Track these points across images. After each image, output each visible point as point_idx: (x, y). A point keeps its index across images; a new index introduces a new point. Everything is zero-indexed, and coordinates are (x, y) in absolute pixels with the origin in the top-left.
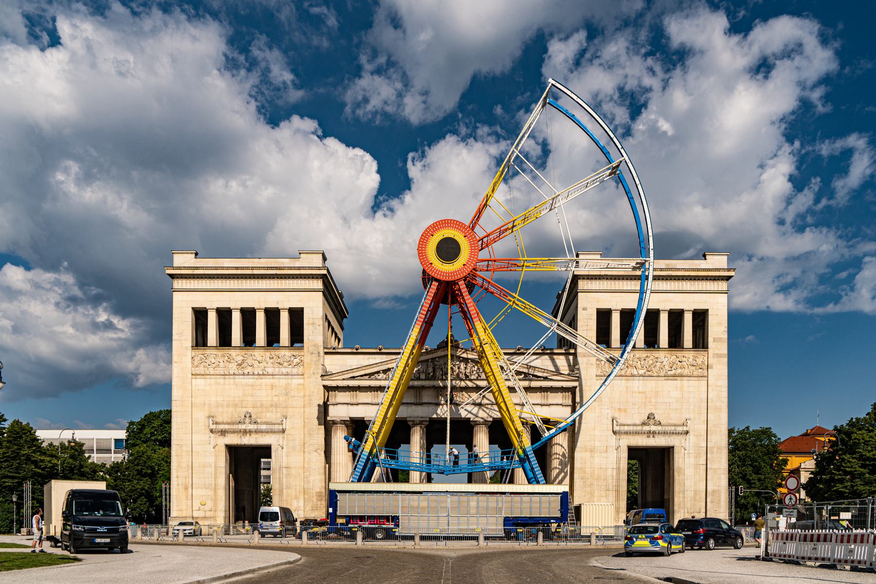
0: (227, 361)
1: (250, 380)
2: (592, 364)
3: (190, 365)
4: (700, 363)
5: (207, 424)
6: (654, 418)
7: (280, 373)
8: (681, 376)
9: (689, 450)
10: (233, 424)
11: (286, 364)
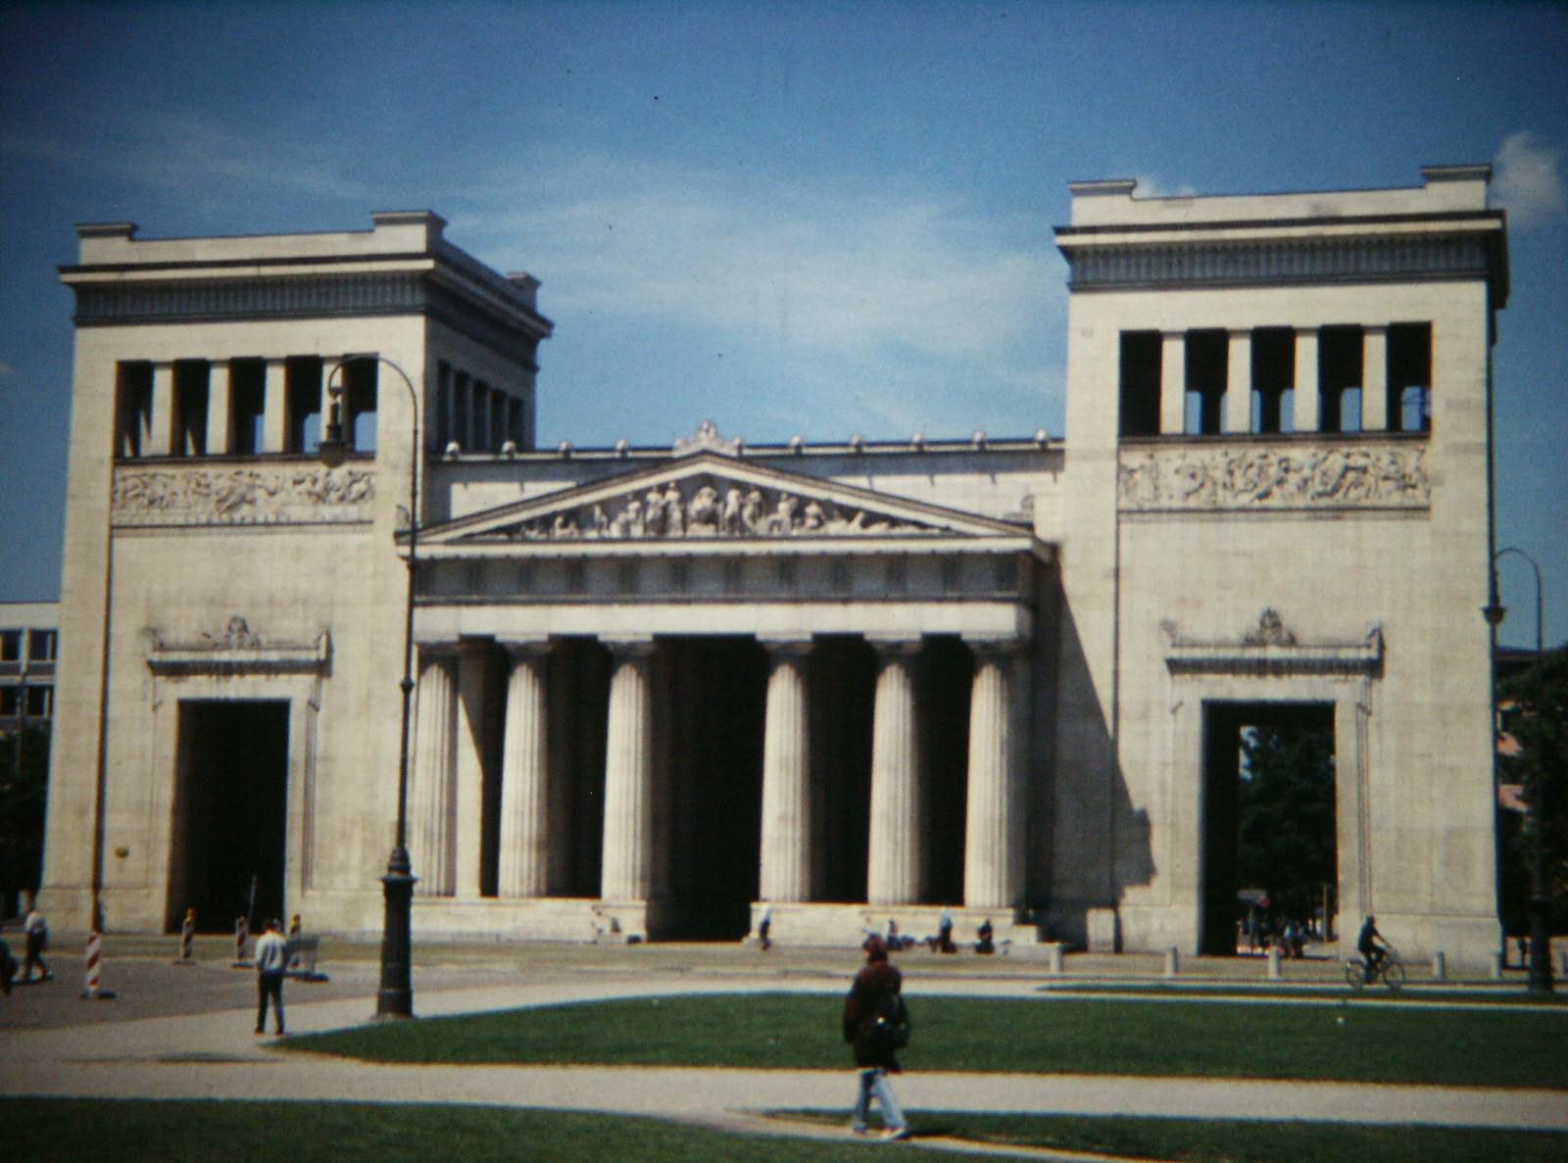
0: (194, 492)
3: (105, 502)
7: (318, 519)
8: (1355, 509)
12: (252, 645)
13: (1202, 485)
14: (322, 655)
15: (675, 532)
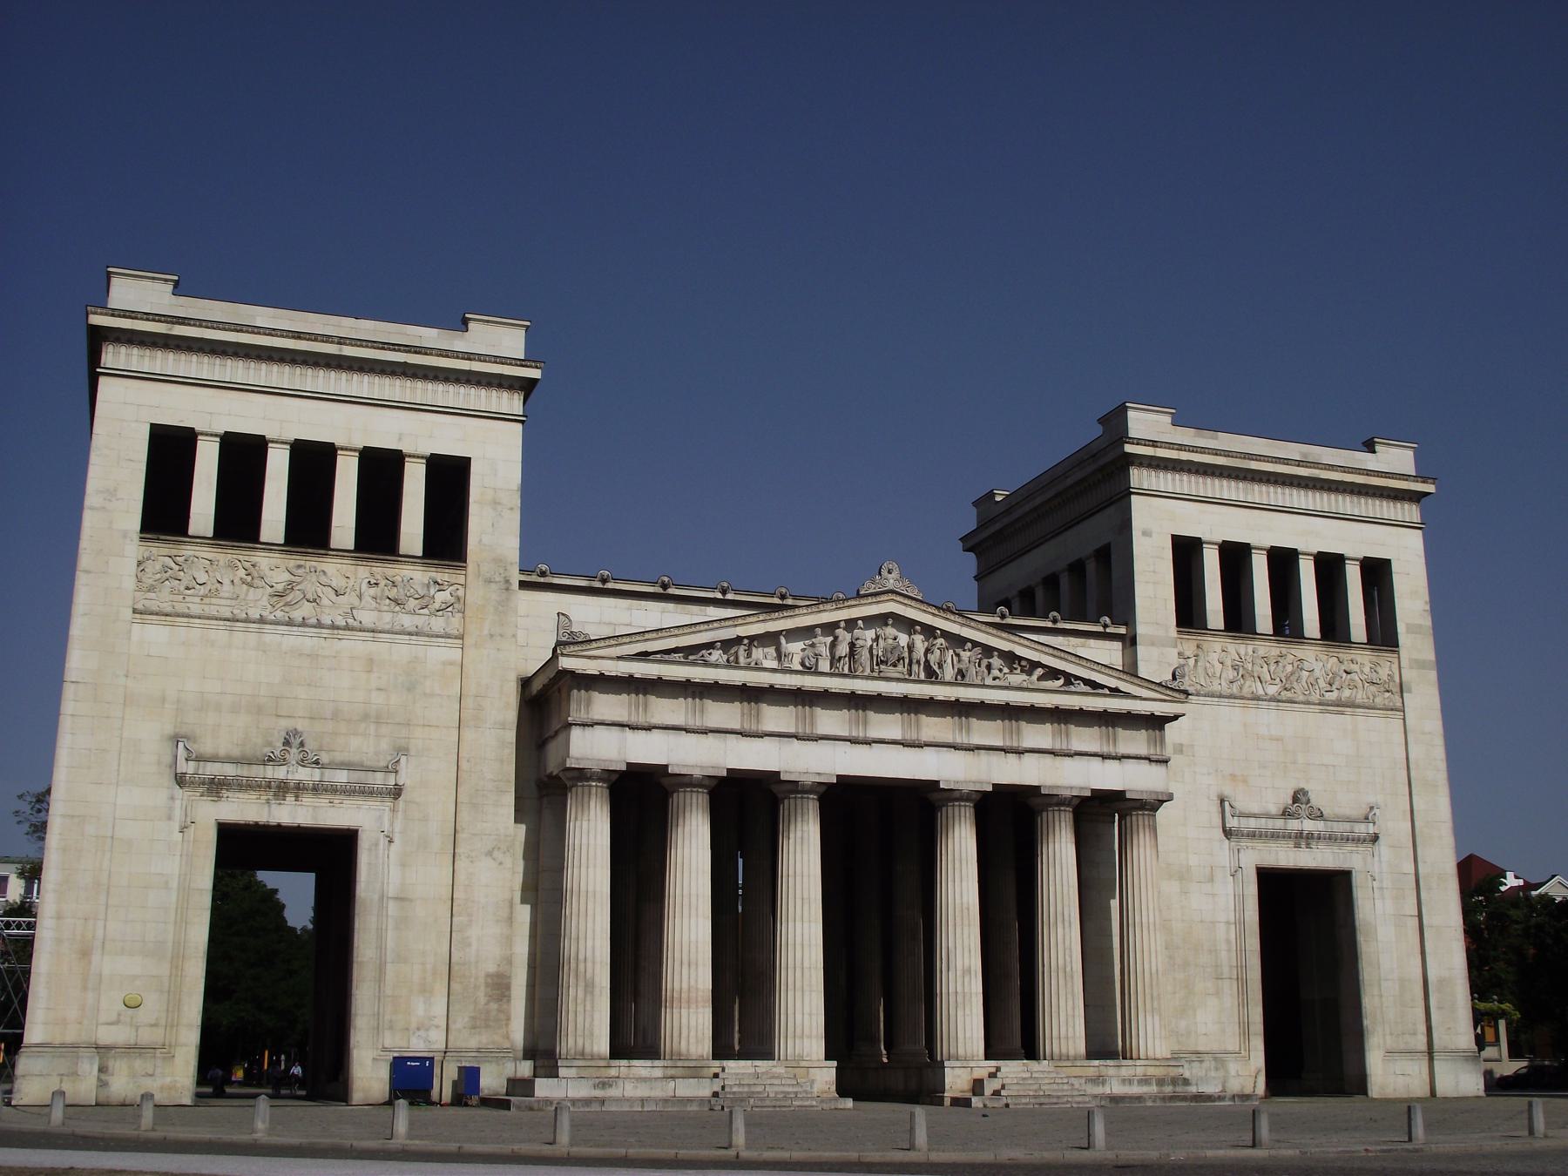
1: (306, 641)
3: (130, 583)
4: (1385, 678)
5: (168, 759)
6: (1308, 801)
7: (397, 628)
8: (1352, 705)
9: (1381, 881)
11: (412, 604)
12: (317, 762)
13: (1242, 676)
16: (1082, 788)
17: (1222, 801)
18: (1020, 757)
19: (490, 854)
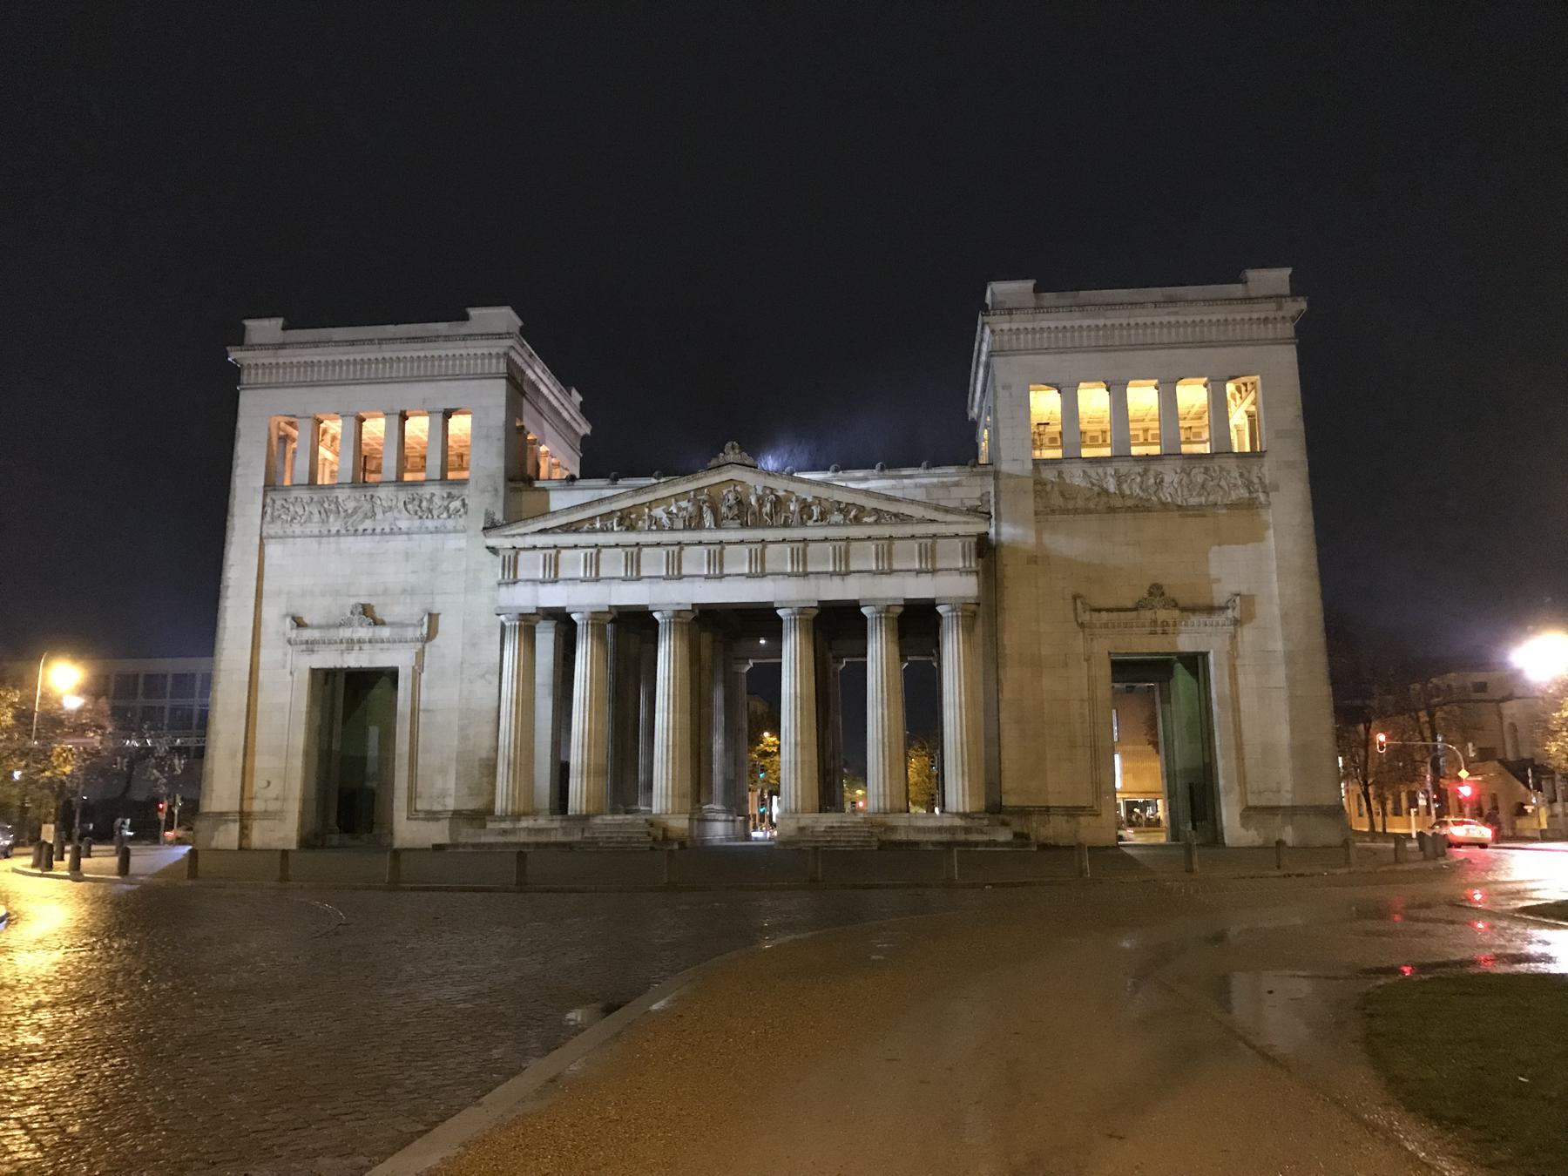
2: (1025, 492)
6: (1163, 594)
10: (328, 626)
14: (425, 630)
15: (708, 520)
16: (895, 599)
17: (1075, 597)
18: (843, 579)
19: (483, 676)
